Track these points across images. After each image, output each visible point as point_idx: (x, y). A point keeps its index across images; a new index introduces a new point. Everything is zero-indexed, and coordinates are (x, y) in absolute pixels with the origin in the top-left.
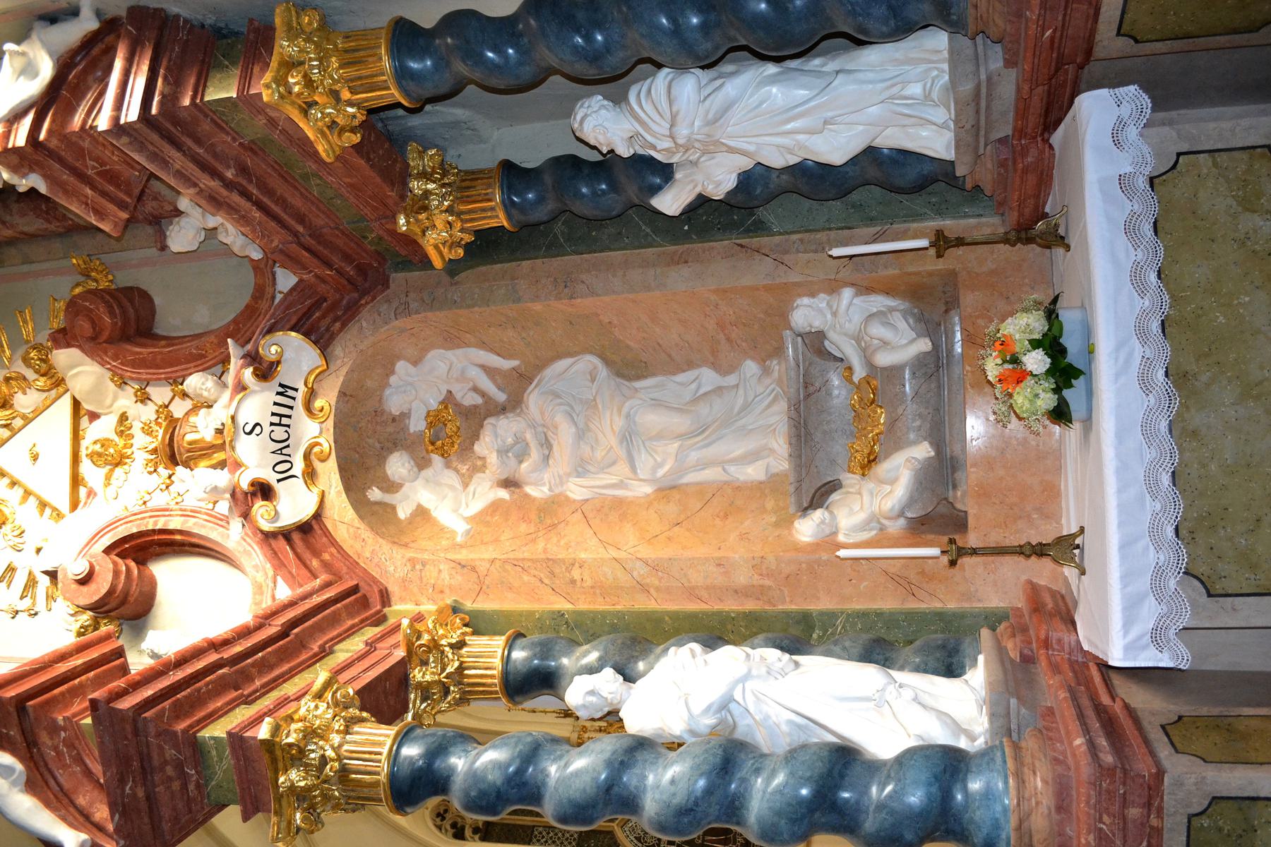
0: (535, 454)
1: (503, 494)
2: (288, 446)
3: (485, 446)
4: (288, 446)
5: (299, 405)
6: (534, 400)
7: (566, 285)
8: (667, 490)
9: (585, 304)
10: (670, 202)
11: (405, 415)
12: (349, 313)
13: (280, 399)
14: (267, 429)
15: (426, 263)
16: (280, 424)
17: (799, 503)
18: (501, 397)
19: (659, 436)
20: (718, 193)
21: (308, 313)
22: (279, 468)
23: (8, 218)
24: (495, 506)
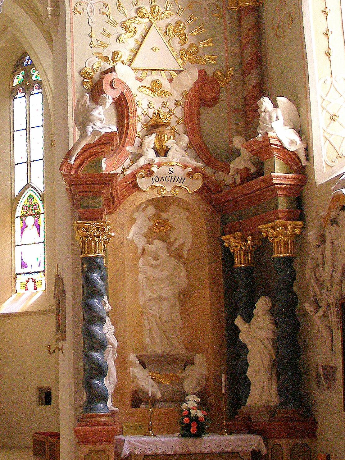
0: (155, 263)
1: (140, 250)
2: (164, 181)
3: (157, 244)
4: (164, 181)
5: (177, 184)
6: (173, 261)
7: (213, 281)
8: (143, 310)
9: (207, 287)
10: (239, 321)
11: (167, 212)
12: (208, 201)
13: (180, 178)
14: (170, 175)
15: (224, 234)
16: (171, 179)
17: (141, 356)
18: (173, 248)
19: (159, 307)
20: (241, 336)
21: (208, 187)
22: (157, 178)
23: (250, 46)
24: (136, 248)
